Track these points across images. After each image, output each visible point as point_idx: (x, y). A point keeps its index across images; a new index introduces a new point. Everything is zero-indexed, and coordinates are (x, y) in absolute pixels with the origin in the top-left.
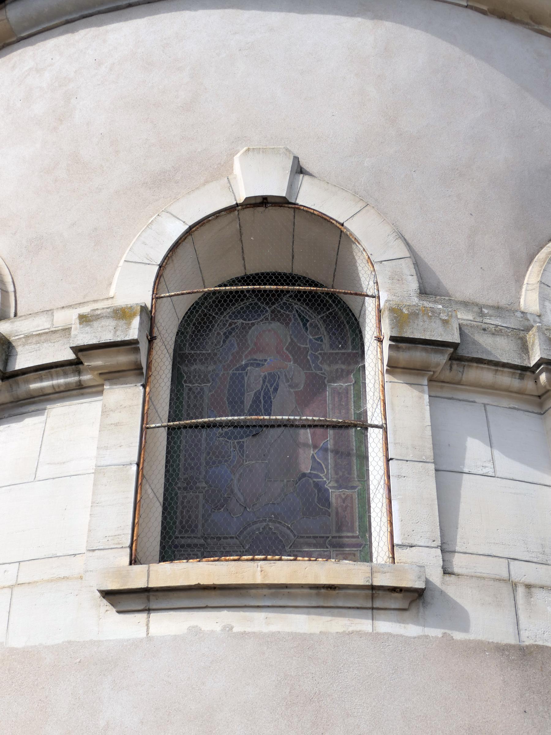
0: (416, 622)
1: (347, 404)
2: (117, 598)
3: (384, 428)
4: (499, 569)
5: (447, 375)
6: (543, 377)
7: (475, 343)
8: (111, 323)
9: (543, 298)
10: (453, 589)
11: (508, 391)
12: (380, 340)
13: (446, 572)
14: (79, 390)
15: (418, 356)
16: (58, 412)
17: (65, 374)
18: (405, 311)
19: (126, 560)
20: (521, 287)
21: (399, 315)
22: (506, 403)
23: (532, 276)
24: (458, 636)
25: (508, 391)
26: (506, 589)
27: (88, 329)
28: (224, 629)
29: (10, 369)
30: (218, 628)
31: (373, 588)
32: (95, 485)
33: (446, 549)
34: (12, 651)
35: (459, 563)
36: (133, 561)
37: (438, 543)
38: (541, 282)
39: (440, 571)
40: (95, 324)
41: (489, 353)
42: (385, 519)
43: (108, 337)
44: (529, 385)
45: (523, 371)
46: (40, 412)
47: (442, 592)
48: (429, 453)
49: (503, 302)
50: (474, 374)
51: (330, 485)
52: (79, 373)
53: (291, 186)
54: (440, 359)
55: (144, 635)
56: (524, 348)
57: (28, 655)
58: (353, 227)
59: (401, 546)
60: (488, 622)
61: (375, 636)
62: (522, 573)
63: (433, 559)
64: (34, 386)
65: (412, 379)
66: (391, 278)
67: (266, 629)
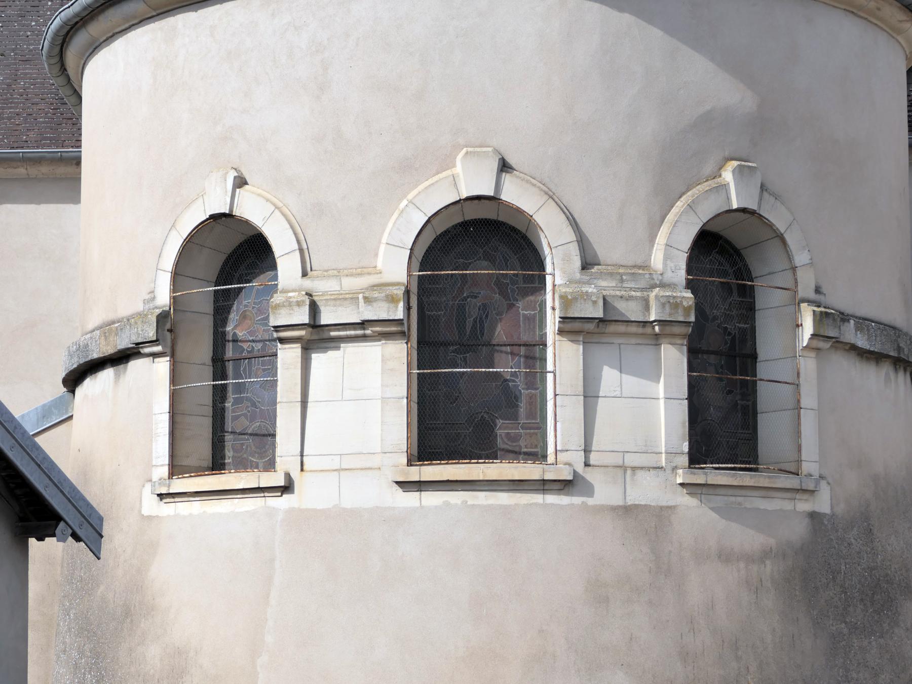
0: (567, 494)
1: (534, 327)
2: (404, 485)
3: (554, 373)
4: (616, 459)
5: (596, 330)
6: (657, 328)
7: (615, 308)
8: (385, 305)
9: (666, 257)
10: (590, 475)
11: (636, 335)
12: (553, 309)
13: (587, 464)
14: (364, 338)
15: (577, 325)
16: (349, 349)
17: (355, 329)
18: (570, 297)
19: (405, 461)
20: (653, 246)
21: (566, 302)
22: (633, 341)
23: (661, 238)
24: (590, 501)
25: (636, 335)
26: (620, 472)
27: (370, 307)
28: (462, 502)
29: (318, 324)
30: (459, 502)
31: (544, 480)
32: (382, 410)
33: (587, 451)
34: (344, 509)
35: (594, 458)
36: (410, 463)
37: (583, 447)
38: (667, 245)
39: (583, 464)
40: (375, 304)
41: (623, 315)
42: (553, 421)
43: (384, 316)
44: (648, 330)
45: (645, 323)
46: (338, 348)
47: (583, 478)
48: (581, 389)
49: (639, 262)
50: (612, 328)
51: (521, 387)
52: (364, 329)
53: (498, 186)
54: (590, 326)
55: (418, 504)
56: (647, 308)
57: (354, 513)
58: (539, 218)
59: (561, 451)
60: (606, 492)
61: (545, 506)
62: (631, 460)
63: (577, 459)
64: (333, 334)
65: (574, 337)
66: (563, 260)
67: (485, 503)
